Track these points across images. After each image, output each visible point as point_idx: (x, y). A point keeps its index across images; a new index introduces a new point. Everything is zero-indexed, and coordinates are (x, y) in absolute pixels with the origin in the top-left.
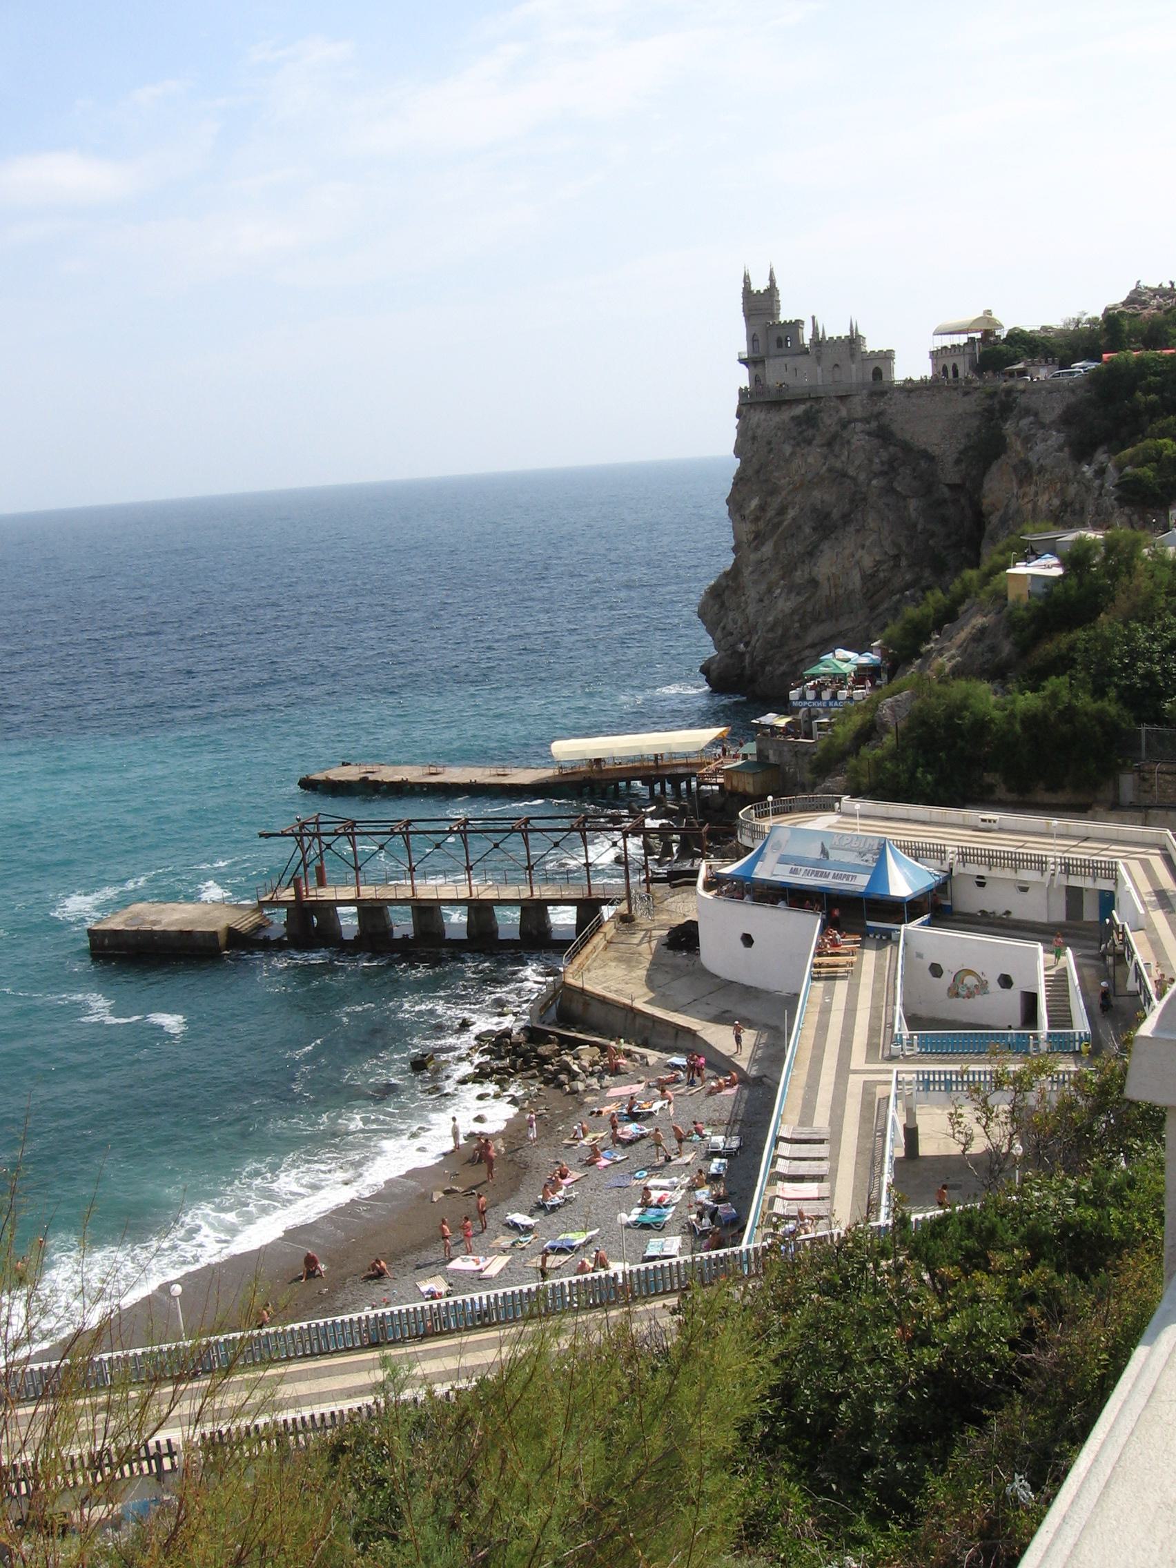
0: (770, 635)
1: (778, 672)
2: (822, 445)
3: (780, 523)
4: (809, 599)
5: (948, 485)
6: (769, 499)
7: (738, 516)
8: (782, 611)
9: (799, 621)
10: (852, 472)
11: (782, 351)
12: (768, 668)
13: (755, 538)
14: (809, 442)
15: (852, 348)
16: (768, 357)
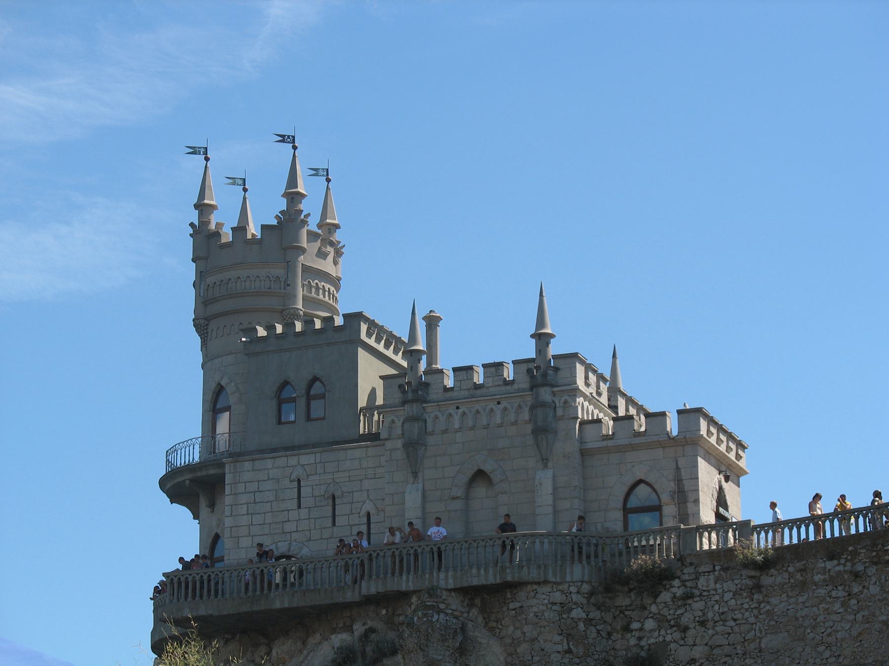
15: (537, 405)
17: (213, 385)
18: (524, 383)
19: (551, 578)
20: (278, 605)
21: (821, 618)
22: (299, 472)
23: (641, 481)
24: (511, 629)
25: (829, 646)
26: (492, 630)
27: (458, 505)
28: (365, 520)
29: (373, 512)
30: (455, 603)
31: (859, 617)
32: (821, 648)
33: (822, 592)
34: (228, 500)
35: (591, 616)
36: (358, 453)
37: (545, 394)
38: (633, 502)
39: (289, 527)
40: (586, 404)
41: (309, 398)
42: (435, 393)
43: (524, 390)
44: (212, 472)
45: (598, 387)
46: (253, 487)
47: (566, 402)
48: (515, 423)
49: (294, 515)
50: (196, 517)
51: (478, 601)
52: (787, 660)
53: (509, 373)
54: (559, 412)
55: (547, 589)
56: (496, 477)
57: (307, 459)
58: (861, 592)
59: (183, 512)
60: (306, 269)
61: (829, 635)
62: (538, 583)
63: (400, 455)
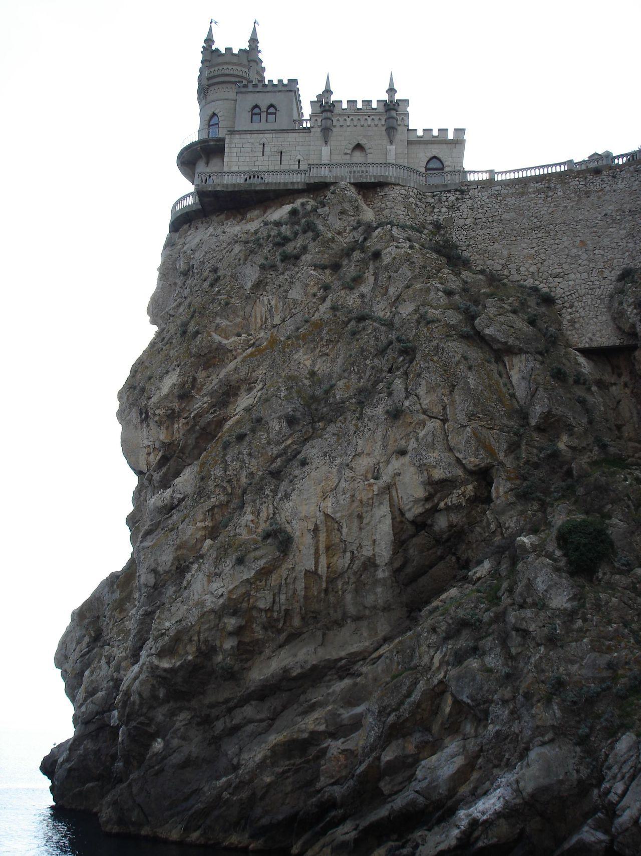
0: (166, 664)
1: (176, 759)
2: (324, 268)
3: (221, 423)
4: (265, 573)
5: (587, 352)
6: (201, 375)
7: (134, 415)
8: (200, 604)
9: (238, 631)
10: (381, 310)
11: (263, 126)
12: (158, 745)
13: (164, 460)
14: (292, 259)
16: (232, 132)
18: (382, 109)
20: (258, 188)
22: (264, 140)
23: (435, 157)
26: (368, 205)
27: (348, 157)
29: (302, 159)
30: (353, 189)
31: (552, 205)
33: (533, 196)
37: (393, 113)
38: (431, 166)
39: (257, 163)
41: (268, 114)
42: (337, 110)
46: (241, 145)
48: (376, 126)
49: (261, 158)
53: (374, 105)
54: (399, 122)
55: (399, 188)
56: (366, 147)
57: (266, 136)
62: (395, 185)
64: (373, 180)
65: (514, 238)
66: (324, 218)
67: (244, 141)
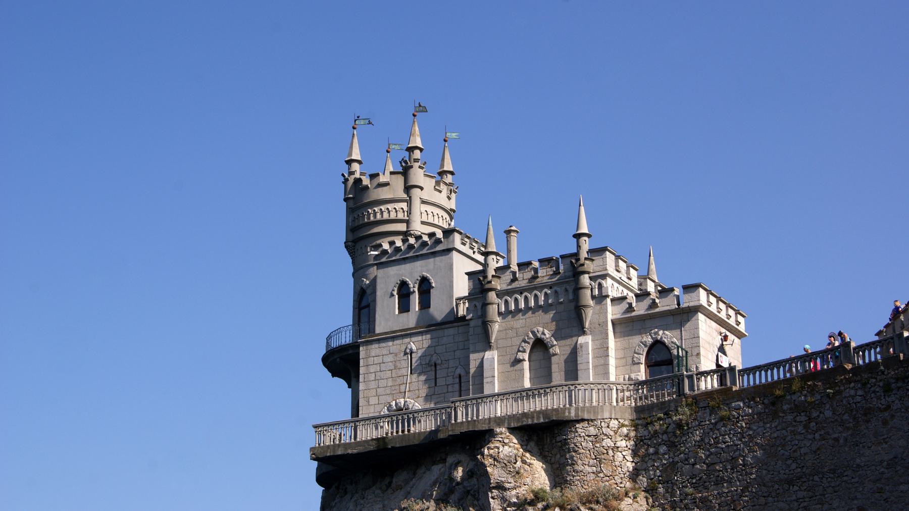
17: (359, 288)
19: (586, 417)
21: (789, 438)
24: (558, 456)
25: (795, 460)
28: (457, 380)
29: (462, 374)
32: (789, 462)
33: (790, 418)
34: (362, 370)
35: (618, 444)
36: (451, 331)
40: (616, 285)
43: (569, 277)
44: (351, 352)
45: (628, 273)
47: (600, 285)
50: (349, 387)
51: (535, 438)
52: (764, 472)
57: (414, 339)
58: (818, 416)
59: (341, 383)
60: (424, 202)
61: (795, 451)
63: (479, 330)
64: (542, 420)
65: (762, 500)
66: (474, 496)
67: (385, 352)
